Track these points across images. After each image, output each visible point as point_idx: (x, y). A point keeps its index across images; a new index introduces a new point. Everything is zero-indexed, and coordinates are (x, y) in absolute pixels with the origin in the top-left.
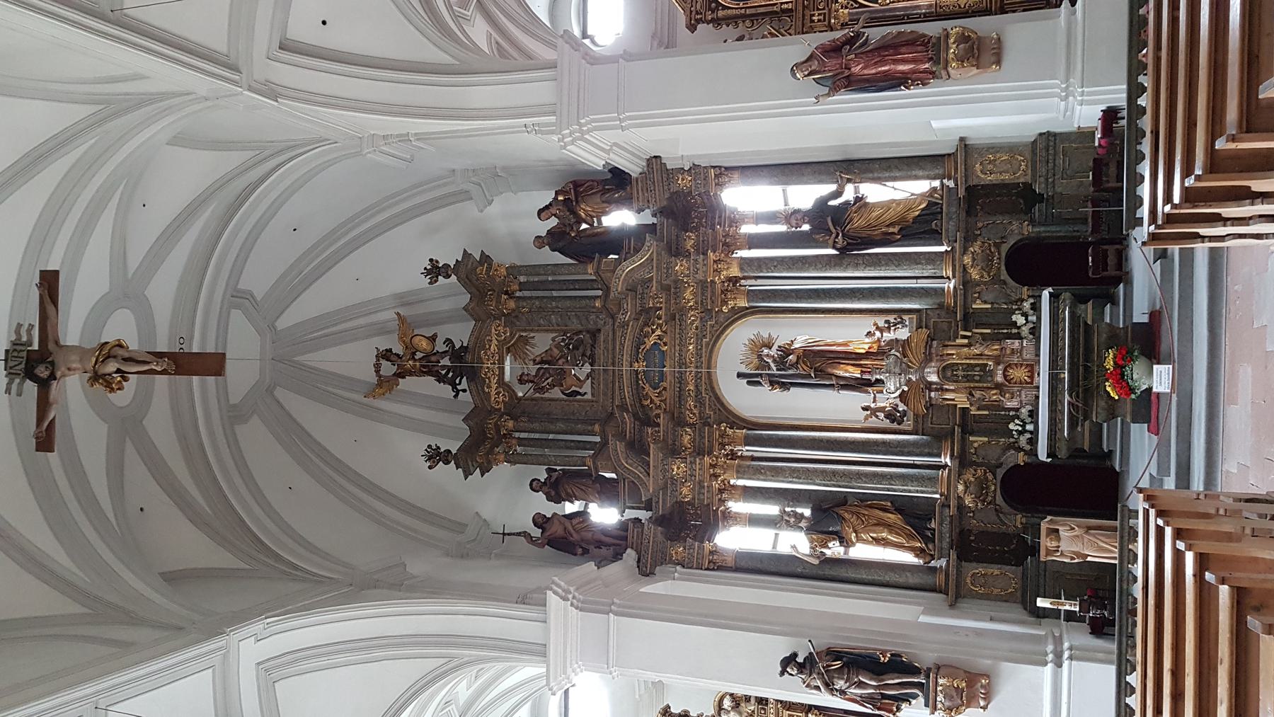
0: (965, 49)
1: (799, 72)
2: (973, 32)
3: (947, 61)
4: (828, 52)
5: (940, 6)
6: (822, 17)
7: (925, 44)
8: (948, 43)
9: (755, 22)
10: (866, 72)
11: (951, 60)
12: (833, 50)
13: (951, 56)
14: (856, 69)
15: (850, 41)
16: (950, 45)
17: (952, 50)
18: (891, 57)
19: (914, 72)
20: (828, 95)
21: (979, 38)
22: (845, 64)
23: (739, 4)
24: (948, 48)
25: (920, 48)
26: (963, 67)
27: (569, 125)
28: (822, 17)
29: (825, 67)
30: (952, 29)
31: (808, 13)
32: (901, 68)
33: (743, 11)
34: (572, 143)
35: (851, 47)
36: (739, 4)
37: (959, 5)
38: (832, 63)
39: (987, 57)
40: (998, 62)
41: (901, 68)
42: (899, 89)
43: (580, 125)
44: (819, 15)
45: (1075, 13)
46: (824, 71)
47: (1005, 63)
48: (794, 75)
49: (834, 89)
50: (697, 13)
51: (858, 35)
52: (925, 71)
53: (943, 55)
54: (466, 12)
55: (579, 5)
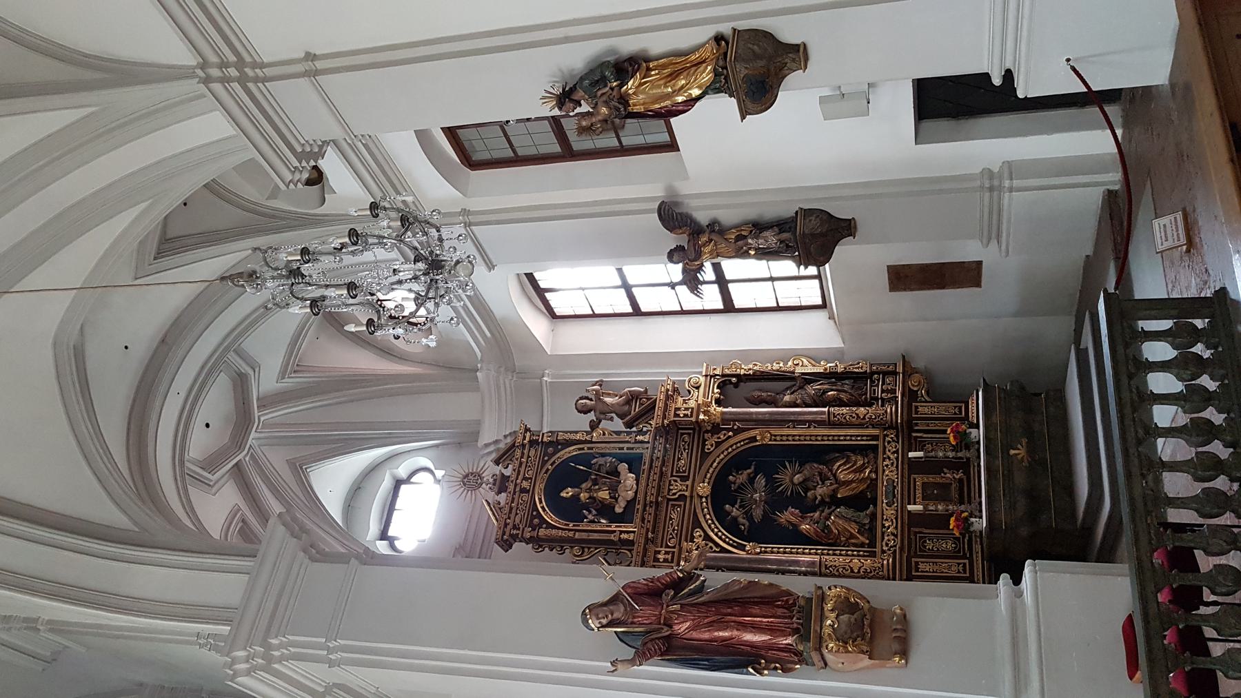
0: (849, 624)
1: (594, 618)
2: (862, 598)
3: (821, 638)
4: (641, 594)
5: (826, 565)
6: (669, 557)
7: (789, 607)
8: (823, 609)
9: (586, 550)
10: (695, 635)
11: (826, 637)
12: (650, 593)
13: (827, 631)
14: (682, 628)
15: (677, 585)
16: (827, 614)
17: (829, 622)
18: (733, 618)
19: (769, 647)
20: (632, 662)
21: (873, 610)
22: (665, 618)
23: (568, 525)
24: (822, 618)
25: (780, 611)
26: (848, 652)
27: (248, 643)
28: (669, 557)
29: (634, 617)
30: (830, 588)
31: (652, 548)
32: (749, 637)
33: (571, 534)
34: (248, 673)
35: (676, 594)
36: (568, 525)
37: (851, 568)
38: (646, 613)
39: (885, 641)
40: (904, 653)
41: (749, 637)
42: (745, 670)
43: (269, 647)
44: (667, 553)
45: (1020, 595)
46: (632, 623)
47: (916, 655)
48: (585, 622)
49: (642, 656)
50: (515, 527)
51: (690, 577)
52: (787, 649)
53: (814, 626)
54: (209, 476)
55: (386, 500)
